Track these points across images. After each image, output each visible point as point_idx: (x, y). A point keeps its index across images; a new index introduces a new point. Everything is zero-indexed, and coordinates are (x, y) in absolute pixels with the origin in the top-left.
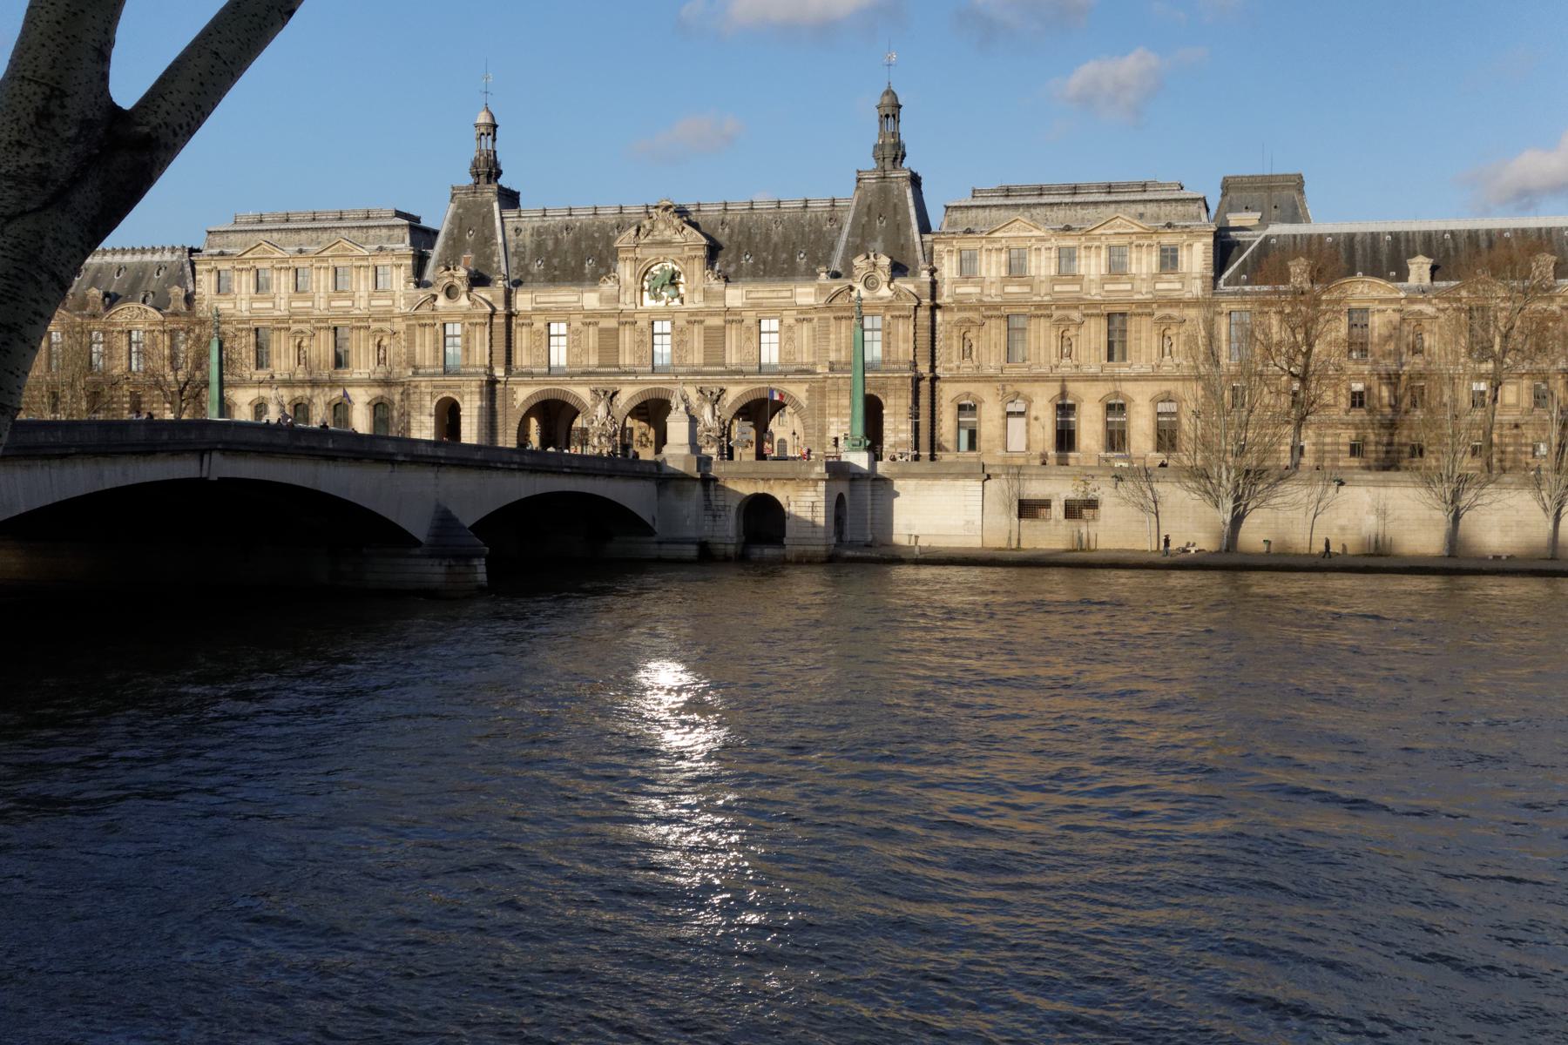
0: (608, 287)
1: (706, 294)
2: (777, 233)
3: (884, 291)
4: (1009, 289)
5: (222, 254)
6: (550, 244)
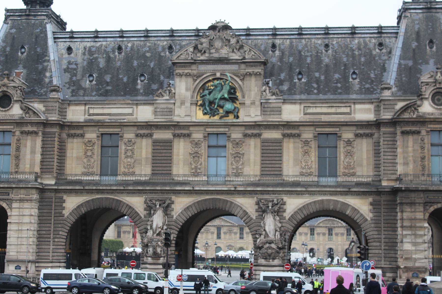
0: (163, 100)
1: (265, 107)
6: (102, 63)
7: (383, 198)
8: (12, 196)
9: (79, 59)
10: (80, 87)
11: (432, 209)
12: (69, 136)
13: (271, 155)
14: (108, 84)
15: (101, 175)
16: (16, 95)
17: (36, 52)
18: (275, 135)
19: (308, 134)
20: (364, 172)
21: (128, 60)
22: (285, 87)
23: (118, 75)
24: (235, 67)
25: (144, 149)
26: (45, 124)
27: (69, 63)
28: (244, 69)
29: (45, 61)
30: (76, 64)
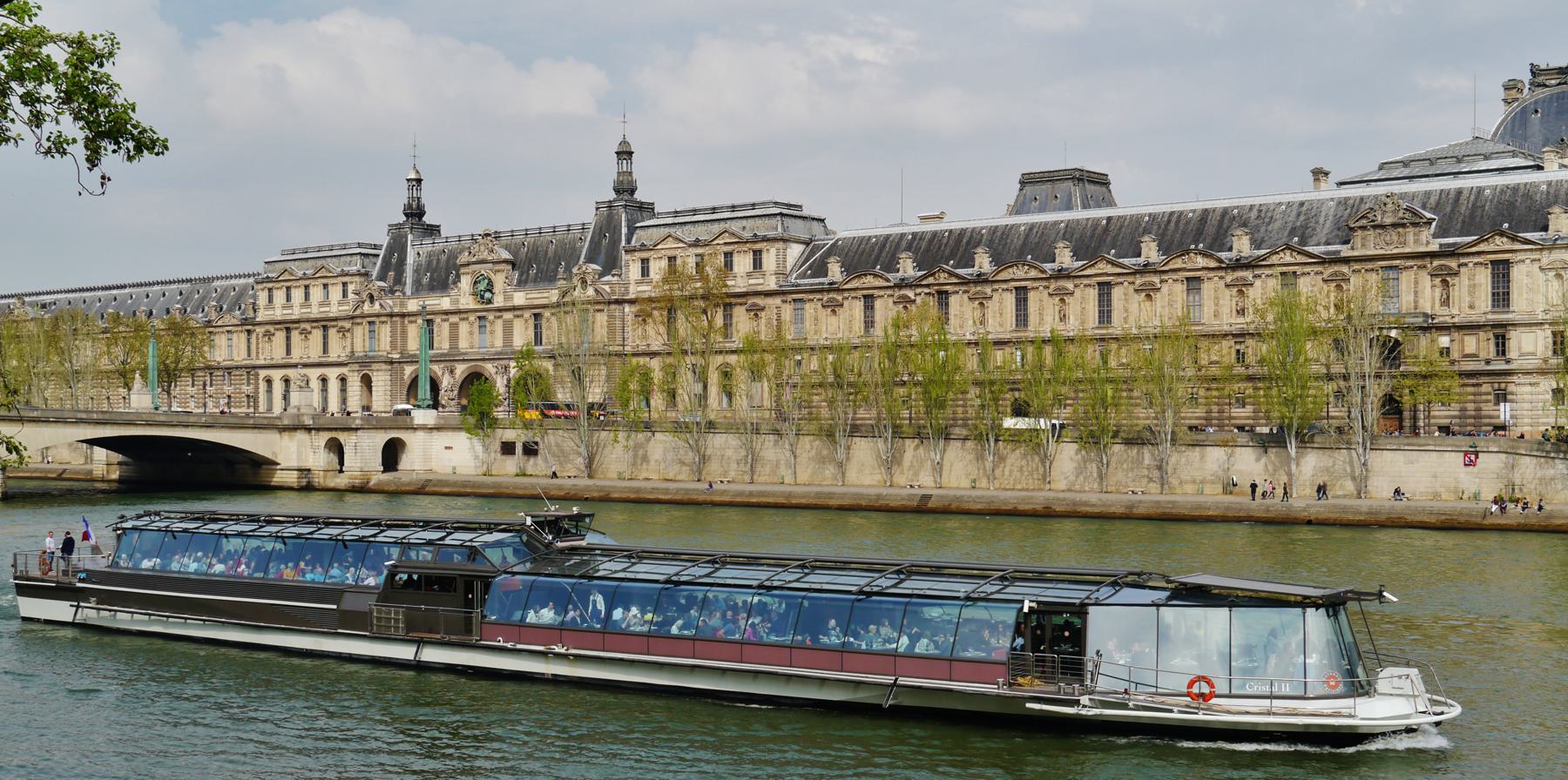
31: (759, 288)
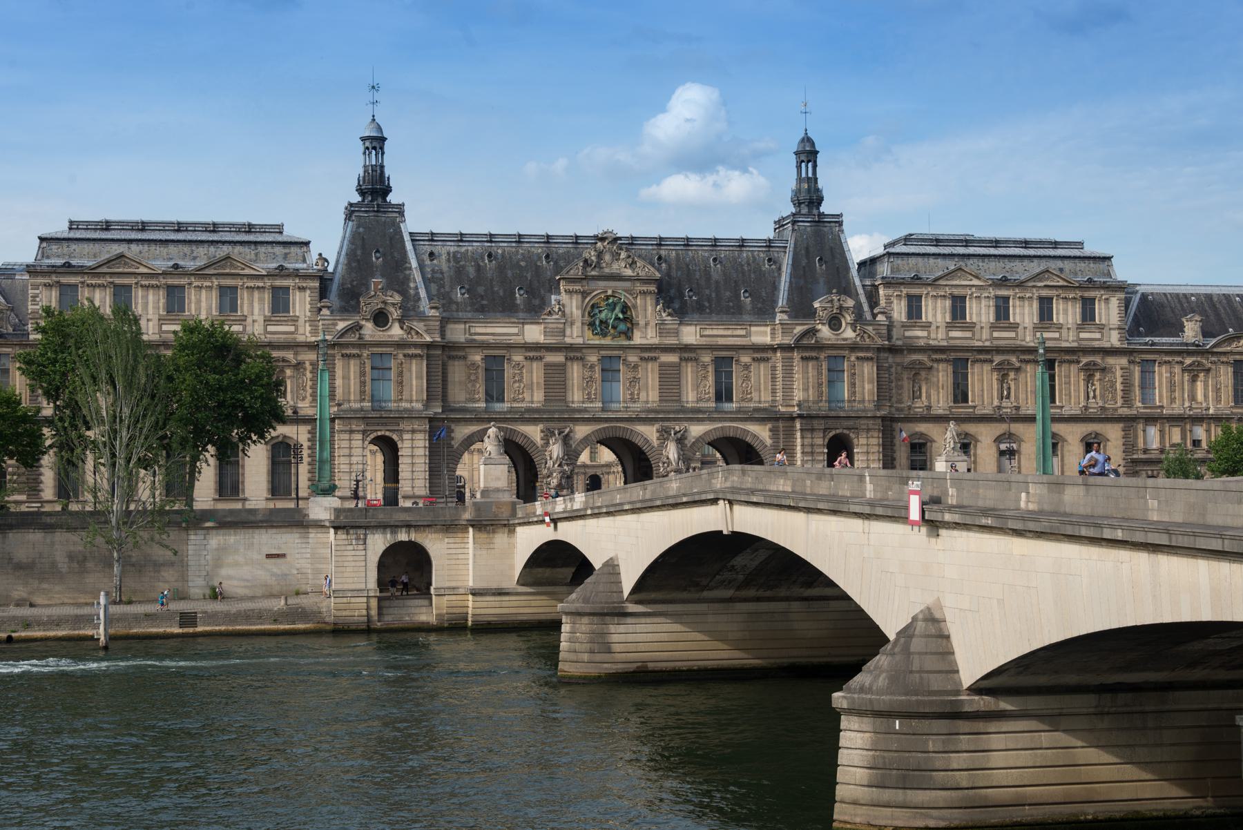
1: (661, 329)
2: (716, 271)
3: (849, 334)
4: (953, 334)
5: (68, 265)
6: (471, 271)
7: (781, 424)
8: (401, 427)
9: (445, 267)
10: (451, 301)
11: (831, 434)
12: (450, 357)
13: (671, 379)
14: (482, 297)
15: (487, 401)
16: (395, 313)
17: (393, 257)
18: (672, 358)
19: (707, 358)
20: (762, 398)
21: (501, 269)
22: (677, 306)
23: (492, 287)
24: (627, 284)
25: (536, 372)
26: (429, 346)
27: (433, 270)
28: (639, 287)
29: (406, 269)
30: (442, 273)
31: (1096, 344)
